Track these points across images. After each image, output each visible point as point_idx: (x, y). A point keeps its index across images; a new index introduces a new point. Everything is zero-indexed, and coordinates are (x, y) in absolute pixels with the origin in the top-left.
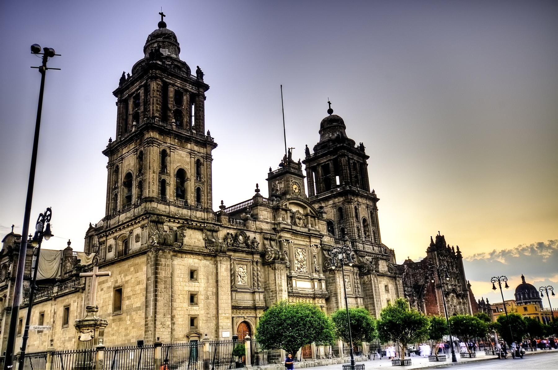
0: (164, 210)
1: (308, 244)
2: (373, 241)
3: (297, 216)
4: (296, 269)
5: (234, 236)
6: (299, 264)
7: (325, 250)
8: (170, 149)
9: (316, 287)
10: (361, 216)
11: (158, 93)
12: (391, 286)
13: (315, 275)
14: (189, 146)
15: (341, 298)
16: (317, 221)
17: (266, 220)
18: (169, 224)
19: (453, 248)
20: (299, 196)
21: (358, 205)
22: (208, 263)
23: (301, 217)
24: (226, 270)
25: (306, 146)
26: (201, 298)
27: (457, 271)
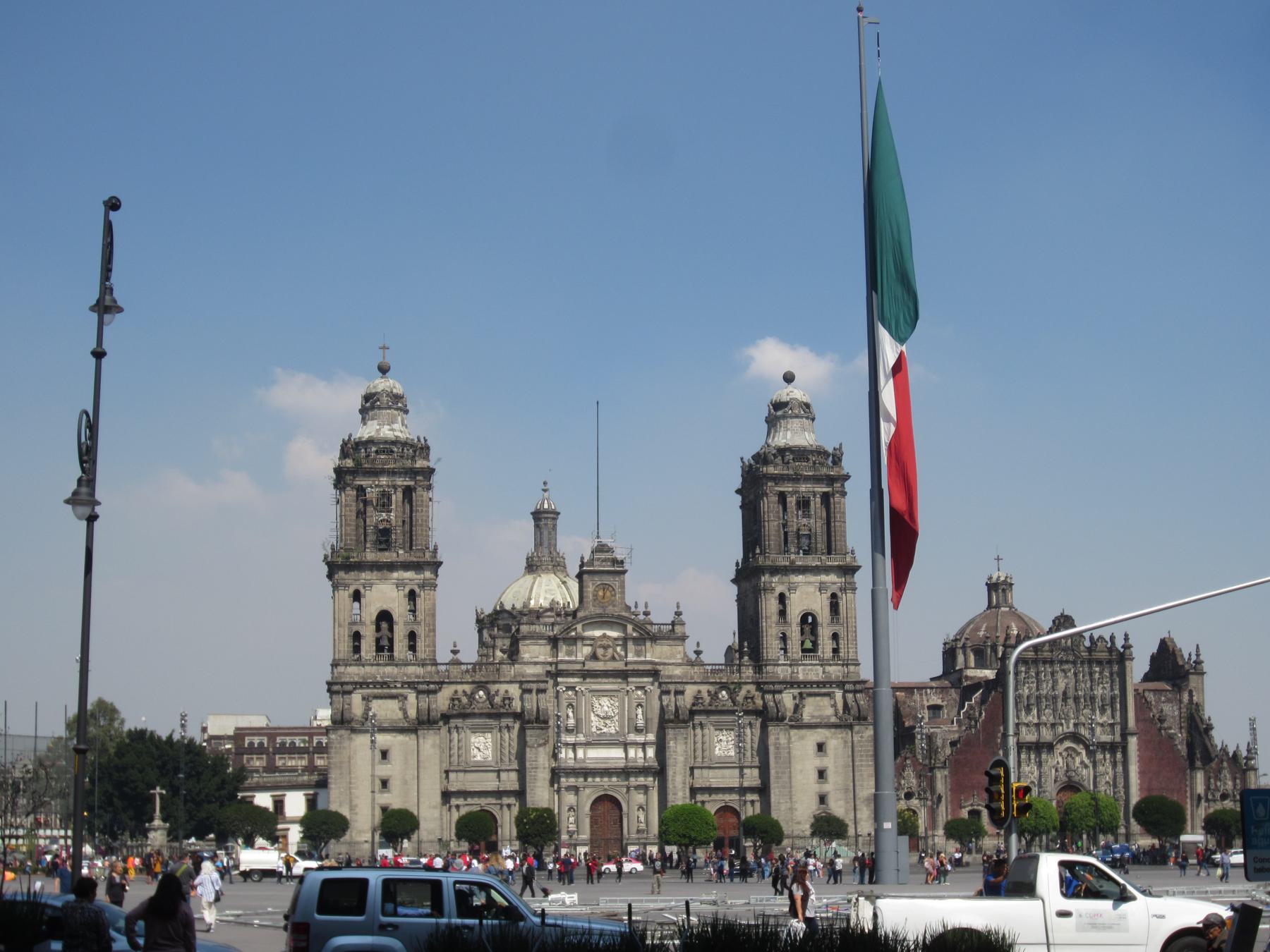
0: (357, 672)
1: (624, 686)
2: (828, 654)
3: (599, 643)
4: (594, 730)
5: (469, 693)
6: (602, 721)
7: (668, 692)
8: (364, 587)
9: (632, 753)
10: (794, 613)
11: (348, 508)
12: (835, 741)
13: (632, 737)
14: (395, 575)
15: (675, 773)
16: (648, 644)
17: (536, 660)
18: (360, 691)
19: (1112, 638)
20: (610, 607)
21: (789, 590)
22: (407, 739)
23: (610, 643)
24: (433, 746)
25: (742, 459)
26: (393, 784)
27: (1112, 690)
